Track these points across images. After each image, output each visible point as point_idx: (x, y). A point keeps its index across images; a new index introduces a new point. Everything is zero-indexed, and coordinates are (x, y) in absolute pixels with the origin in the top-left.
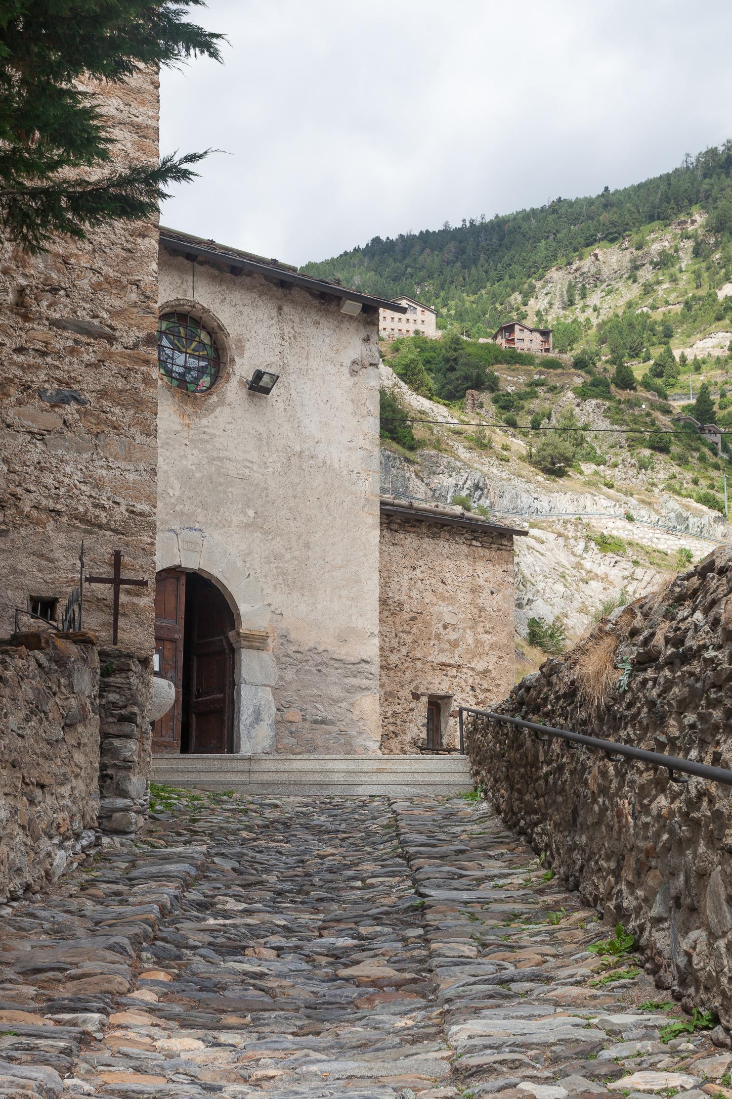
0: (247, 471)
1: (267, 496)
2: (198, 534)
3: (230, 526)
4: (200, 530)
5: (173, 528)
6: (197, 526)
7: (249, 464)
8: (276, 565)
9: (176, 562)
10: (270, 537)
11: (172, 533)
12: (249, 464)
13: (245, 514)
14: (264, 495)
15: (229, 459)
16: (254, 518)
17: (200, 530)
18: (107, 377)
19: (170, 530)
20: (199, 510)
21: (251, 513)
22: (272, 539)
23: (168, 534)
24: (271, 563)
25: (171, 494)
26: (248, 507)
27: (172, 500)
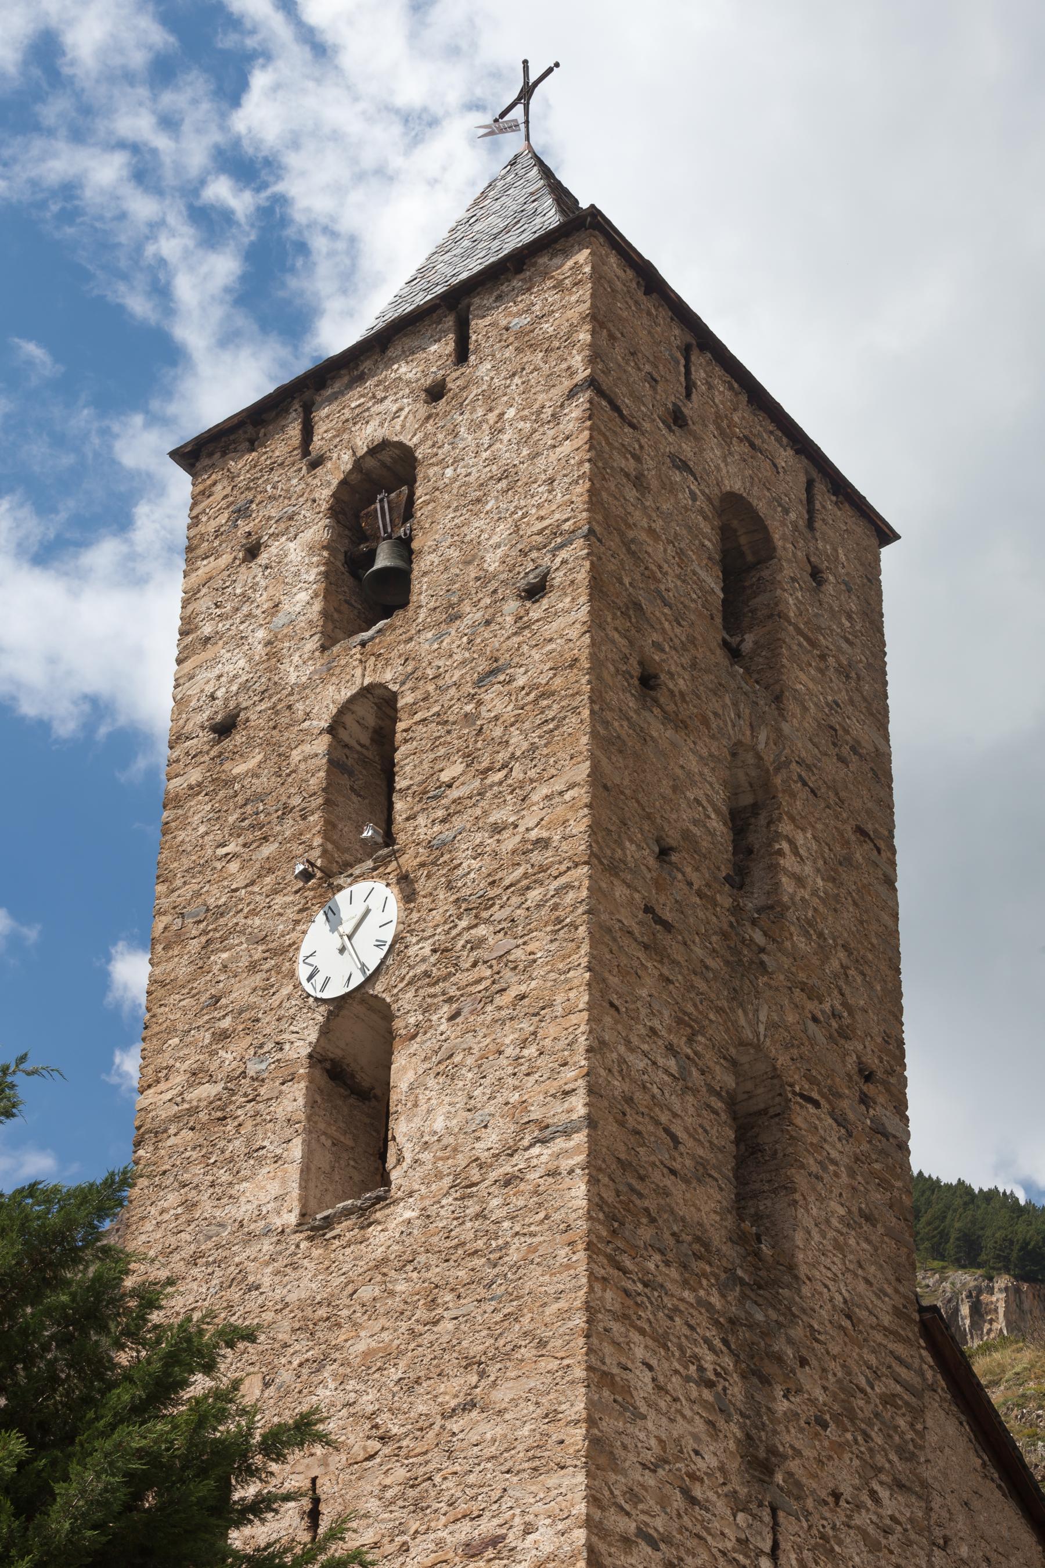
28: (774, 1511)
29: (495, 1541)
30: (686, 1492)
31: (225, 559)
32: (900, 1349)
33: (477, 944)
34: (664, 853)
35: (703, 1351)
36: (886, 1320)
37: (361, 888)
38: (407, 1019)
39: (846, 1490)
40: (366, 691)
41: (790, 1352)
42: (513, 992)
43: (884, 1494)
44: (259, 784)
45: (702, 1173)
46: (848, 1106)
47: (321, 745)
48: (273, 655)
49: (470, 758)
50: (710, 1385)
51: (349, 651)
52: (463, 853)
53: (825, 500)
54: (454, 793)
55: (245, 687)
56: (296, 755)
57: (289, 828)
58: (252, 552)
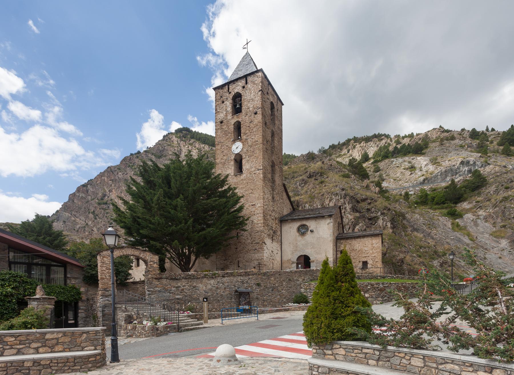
18: (259, 247)
31: (220, 103)
33: (251, 150)
37: (238, 143)
38: (244, 156)
40: (237, 121)
44: (226, 129)
47: (233, 126)
48: (226, 115)
49: (249, 131)
51: (235, 117)
52: (249, 140)
53: (278, 101)
54: (248, 134)
55: (223, 118)
56: (230, 127)
57: (230, 135)
58: (223, 102)
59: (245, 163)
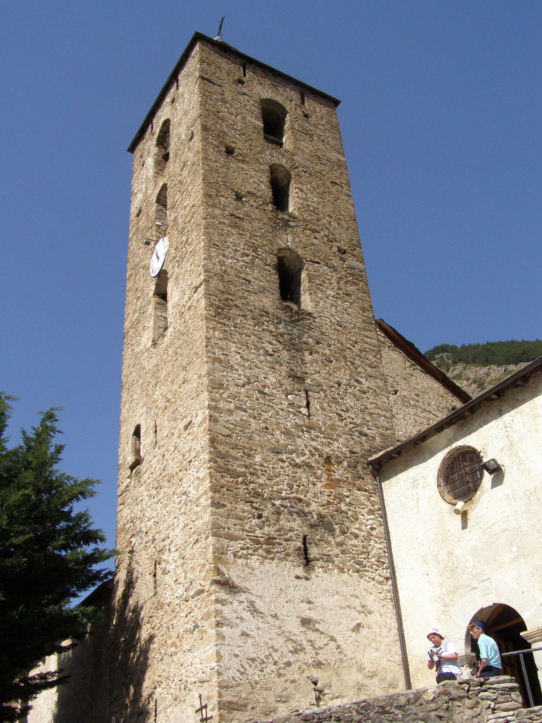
0: (506, 524)
1: (522, 532)
2: (488, 581)
3: (504, 566)
4: (488, 579)
5: (473, 586)
6: (486, 577)
7: (506, 519)
8: (538, 574)
9: (480, 608)
10: (530, 557)
11: (474, 590)
12: (506, 519)
13: (511, 552)
14: (519, 532)
15: (495, 524)
16: (517, 551)
17: (488, 579)
19: (472, 589)
20: (485, 566)
21: (515, 549)
22: (532, 559)
23: (472, 592)
24: (535, 575)
25: (469, 566)
26: (512, 546)
27: (470, 570)
28: (306, 392)
29: (191, 422)
30: (261, 392)
32: (368, 333)
34: (239, 198)
35: (266, 345)
36: (358, 325)
39: (344, 382)
41: (311, 340)
42: (189, 252)
43: (363, 380)
45: (263, 290)
46: (336, 262)
50: (271, 355)
59: (173, 290)
